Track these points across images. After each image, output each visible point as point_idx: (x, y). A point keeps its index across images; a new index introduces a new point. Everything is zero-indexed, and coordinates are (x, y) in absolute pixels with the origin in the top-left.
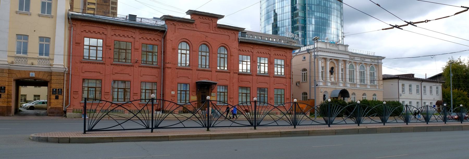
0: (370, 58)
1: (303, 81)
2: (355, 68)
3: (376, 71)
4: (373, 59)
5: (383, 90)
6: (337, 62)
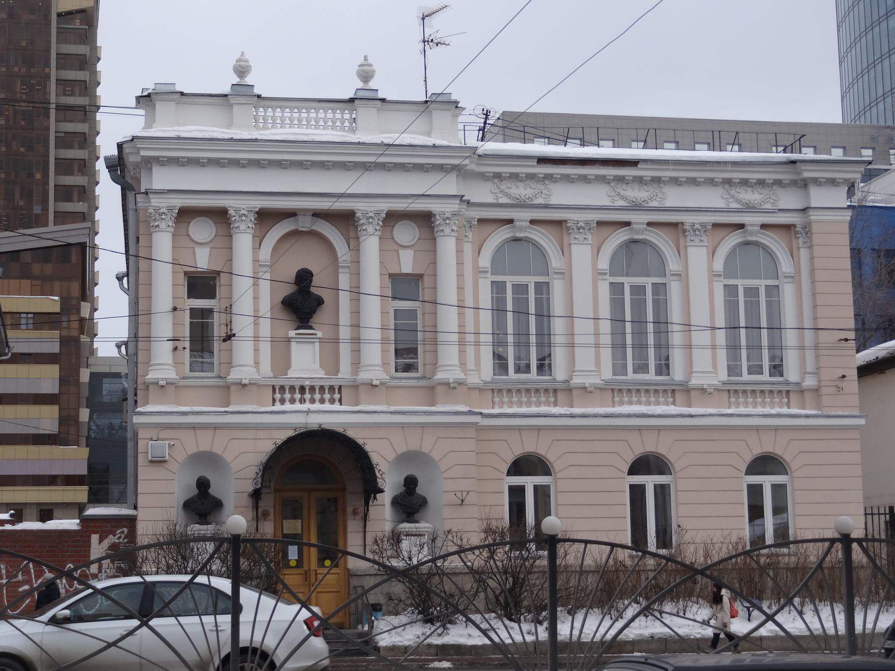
0: (711, 182)
2: (556, 262)
3: (795, 278)
4: (745, 183)
5: (862, 422)
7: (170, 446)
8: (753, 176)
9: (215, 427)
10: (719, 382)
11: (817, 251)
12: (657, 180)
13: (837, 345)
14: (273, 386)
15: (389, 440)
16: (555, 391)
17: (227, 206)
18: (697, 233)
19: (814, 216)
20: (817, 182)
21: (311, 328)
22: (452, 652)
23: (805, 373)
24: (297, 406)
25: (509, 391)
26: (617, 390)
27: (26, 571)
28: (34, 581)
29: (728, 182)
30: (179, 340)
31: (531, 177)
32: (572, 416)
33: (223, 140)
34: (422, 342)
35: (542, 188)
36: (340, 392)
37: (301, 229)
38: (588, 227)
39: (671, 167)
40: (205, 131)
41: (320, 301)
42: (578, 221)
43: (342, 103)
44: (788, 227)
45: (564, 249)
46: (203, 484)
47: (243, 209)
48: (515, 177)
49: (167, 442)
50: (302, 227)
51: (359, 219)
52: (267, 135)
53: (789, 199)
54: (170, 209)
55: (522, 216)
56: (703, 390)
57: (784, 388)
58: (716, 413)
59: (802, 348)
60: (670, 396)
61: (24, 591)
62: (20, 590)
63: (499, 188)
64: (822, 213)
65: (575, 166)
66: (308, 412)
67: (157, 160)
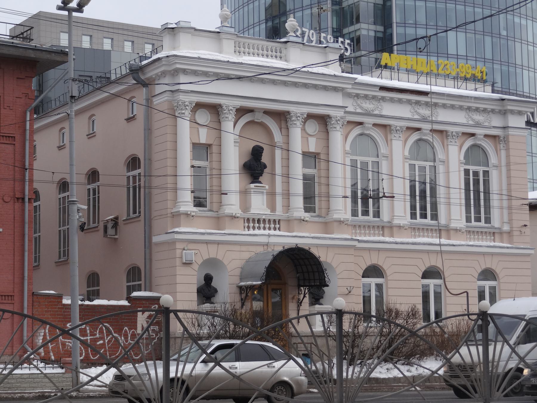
0: (461, 108)
1: (128, 215)
2: (383, 150)
4: (477, 110)
5: (532, 252)
6: (283, 125)
7: (196, 254)
8: (482, 106)
9: (218, 243)
10: (408, 222)
11: (512, 152)
12: (436, 105)
13: (521, 207)
14: (244, 218)
15: (478, 262)
16: (383, 227)
17: (222, 103)
18: (454, 137)
19: (511, 132)
20: (512, 112)
21: (260, 183)
22: (374, 382)
23: (503, 223)
24: (262, 232)
25: (360, 226)
26: (426, 229)
27: (101, 332)
28: (106, 337)
29: (469, 109)
30: (348, 197)
31: (374, 98)
32: (396, 243)
33: (224, 62)
34: (462, 205)
35: (378, 105)
36: (279, 224)
37: (256, 120)
38: (401, 130)
39: (445, 98)
40: (213, 55)
41: (265, 167)
42: (397, 126)
43: (280, 43)
44: (494, 137)
45: (445, 147)
46: (208, 279)
47: (231, 106)
48: (366, 97)
49: (193, 251)
50: (257, 119)
51: (292, 116)
52: (247, 61)
53: (497, 121)
54: (191, 103)
55: (369, 121)
56: (400, 227)
57: (492, 231)
58: (465, 244)
59: (501, 208)
60: (381, 230)
61: (100, 344)
62: (98, 343)
63: (357, 103)
64: (515, 131)
65: (397, 93)
66: (269, 236)
67: (185, 72)
